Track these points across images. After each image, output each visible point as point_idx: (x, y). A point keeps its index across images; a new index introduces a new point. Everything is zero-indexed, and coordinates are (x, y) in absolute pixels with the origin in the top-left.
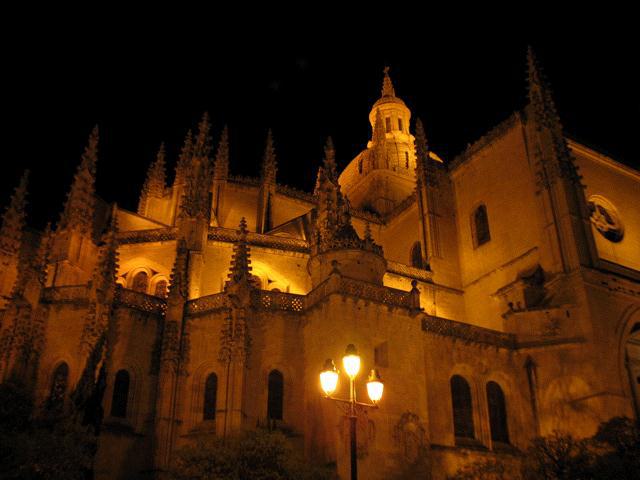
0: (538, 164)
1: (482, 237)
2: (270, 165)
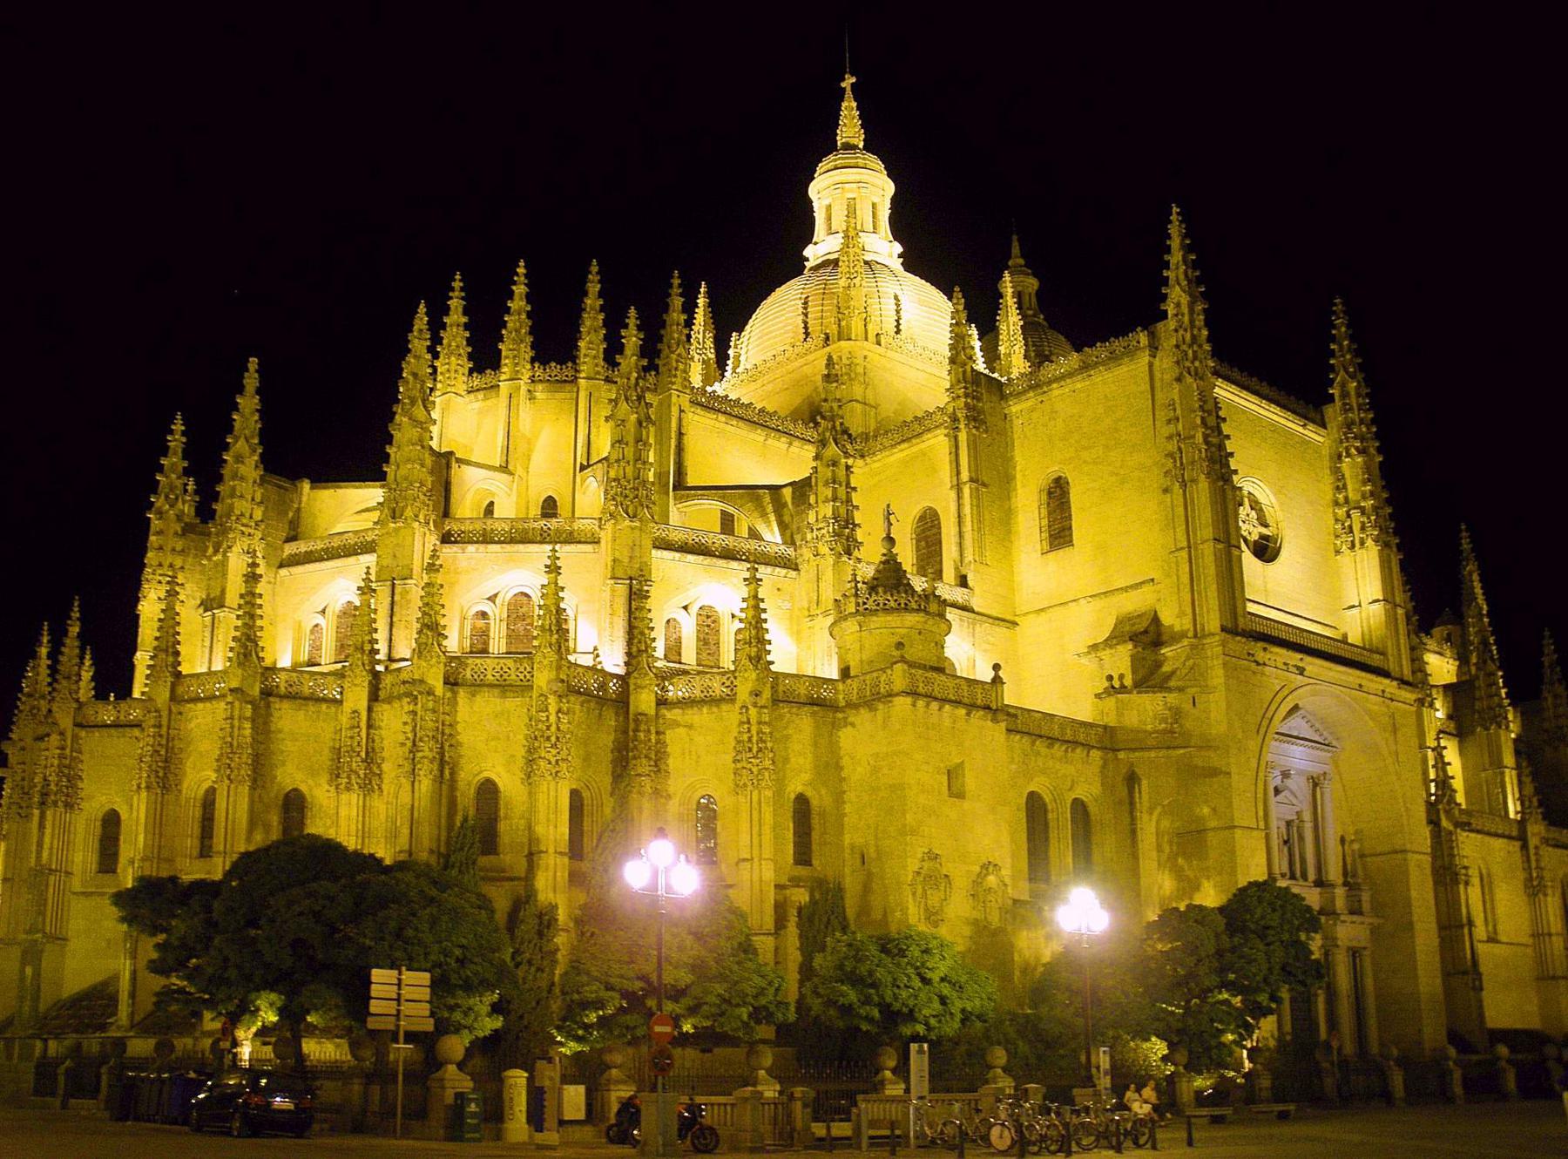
0: (1170, 438)
1: (1059, 535)
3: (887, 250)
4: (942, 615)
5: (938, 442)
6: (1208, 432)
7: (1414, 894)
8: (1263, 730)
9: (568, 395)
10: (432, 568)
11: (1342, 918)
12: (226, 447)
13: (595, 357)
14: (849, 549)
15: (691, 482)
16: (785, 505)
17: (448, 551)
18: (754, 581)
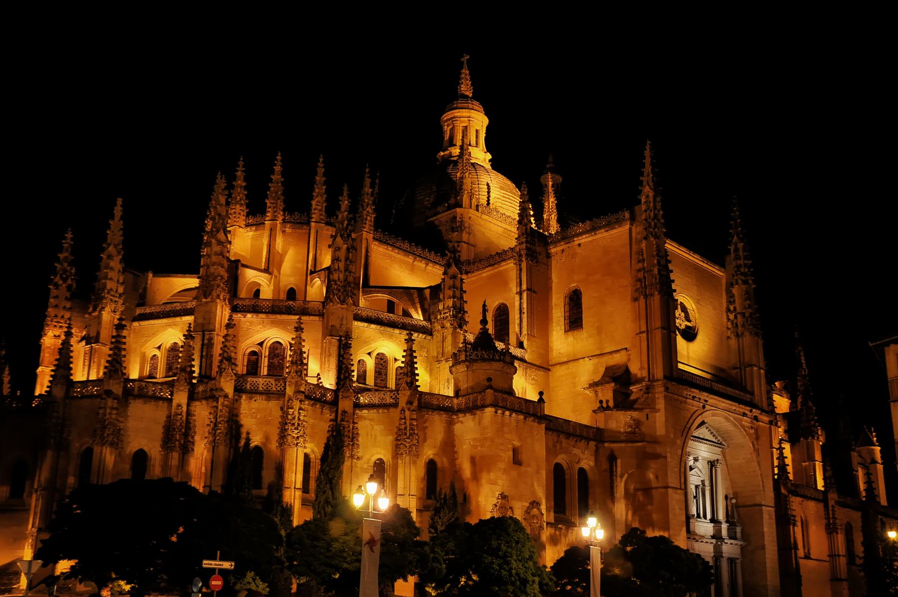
0: (639, 270)
1: (574, 322)
2: (369, 209)
3: (481, 155)
4: (512, 364)
5: (510, 266)
6: (661, 268)
7: (765, 529)
8: (685, 434)
9: (304, 231)
10: (229, 326)
11: (726, 541)
13: (320, 210)
14: (461, 323)
15: (372, 284)
16: (426, 298)
17: (238, 316)
18: (410, 341)
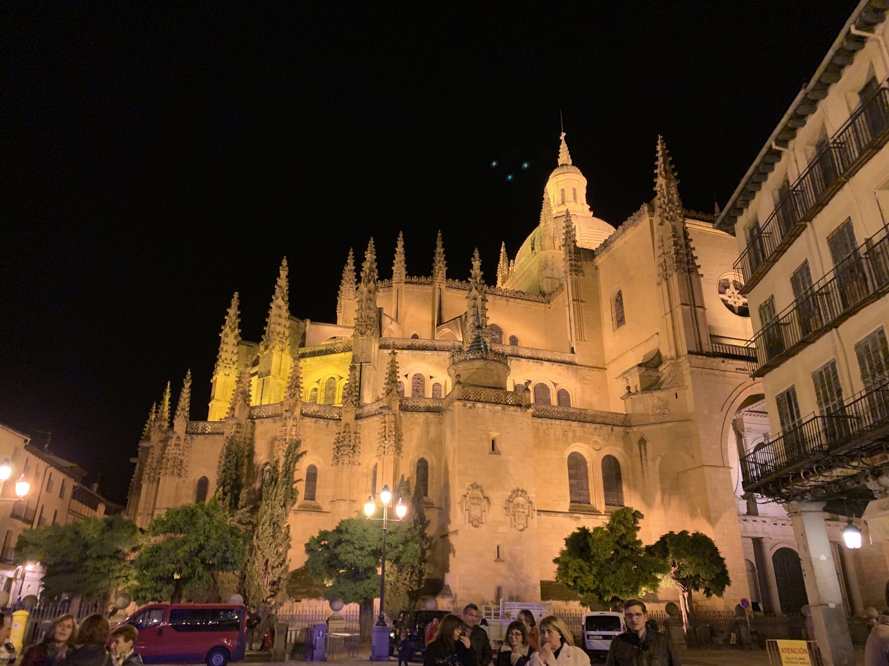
1: (620, 321)
2: (440, 264)
6: (678, 248)
12: (221, 331)
